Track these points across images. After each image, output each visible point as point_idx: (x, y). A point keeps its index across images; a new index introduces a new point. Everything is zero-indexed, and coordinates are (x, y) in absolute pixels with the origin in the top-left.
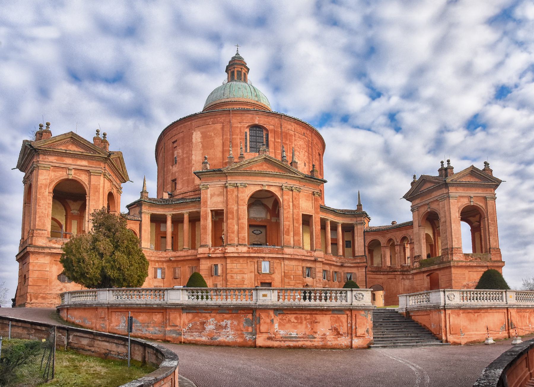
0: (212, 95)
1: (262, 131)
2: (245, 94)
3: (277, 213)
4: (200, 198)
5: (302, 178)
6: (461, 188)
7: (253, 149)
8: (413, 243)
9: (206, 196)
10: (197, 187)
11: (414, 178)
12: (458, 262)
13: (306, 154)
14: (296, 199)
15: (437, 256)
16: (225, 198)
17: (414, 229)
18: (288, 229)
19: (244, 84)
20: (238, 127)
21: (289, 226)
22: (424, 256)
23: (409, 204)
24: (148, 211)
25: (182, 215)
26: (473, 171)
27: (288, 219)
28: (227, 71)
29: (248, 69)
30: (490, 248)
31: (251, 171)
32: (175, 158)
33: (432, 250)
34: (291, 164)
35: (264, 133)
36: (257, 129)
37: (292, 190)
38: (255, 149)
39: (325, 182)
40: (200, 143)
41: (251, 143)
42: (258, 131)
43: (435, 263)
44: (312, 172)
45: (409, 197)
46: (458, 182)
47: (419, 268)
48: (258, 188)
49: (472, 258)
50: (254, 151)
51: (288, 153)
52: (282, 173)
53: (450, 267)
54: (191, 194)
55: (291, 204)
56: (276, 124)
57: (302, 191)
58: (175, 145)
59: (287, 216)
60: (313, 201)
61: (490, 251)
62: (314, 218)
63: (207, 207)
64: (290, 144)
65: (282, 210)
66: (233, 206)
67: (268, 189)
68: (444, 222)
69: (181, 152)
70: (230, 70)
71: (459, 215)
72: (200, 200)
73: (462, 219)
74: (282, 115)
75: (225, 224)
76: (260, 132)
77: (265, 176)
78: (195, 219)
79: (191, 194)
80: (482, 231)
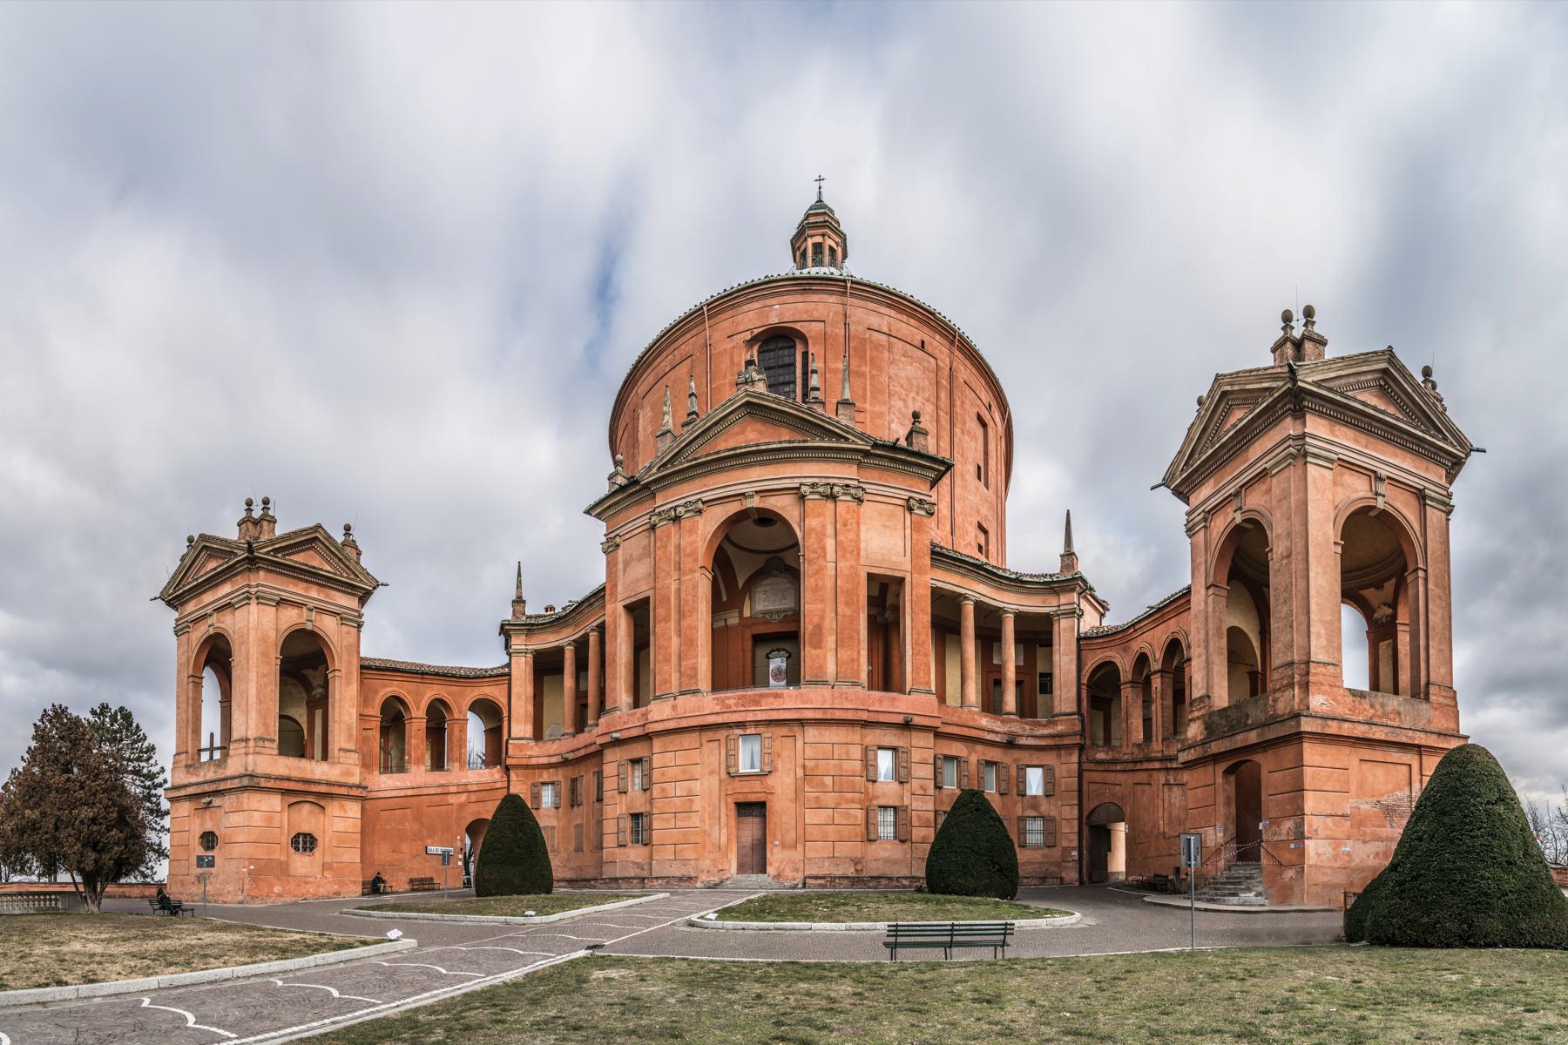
1: (794, 347)
18: (819, 627)
20: (725, 350)
21: (822, 617)
27: (820, 593)
36: (780, 345)
42: (782, 348)
51: (865, 402)
59: (817, 585)
60: (908, 531)
64: (874, 373)
68: (1283, 558)
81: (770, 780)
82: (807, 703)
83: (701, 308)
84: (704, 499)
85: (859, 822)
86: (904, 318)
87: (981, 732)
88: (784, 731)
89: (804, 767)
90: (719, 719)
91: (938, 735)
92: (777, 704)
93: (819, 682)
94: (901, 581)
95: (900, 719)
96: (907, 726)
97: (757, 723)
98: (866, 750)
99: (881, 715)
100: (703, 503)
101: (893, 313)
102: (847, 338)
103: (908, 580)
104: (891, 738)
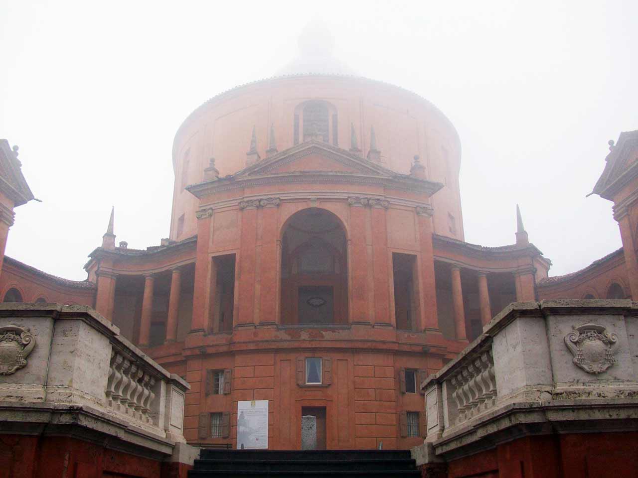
24: (111, 271)
48: (301, 207)
75: (236, 284)
81: (329, 392)
84: (282, 198)
85: (395, 423)
89: (354, 382)
94: (415, 256)
103: (418, 256)
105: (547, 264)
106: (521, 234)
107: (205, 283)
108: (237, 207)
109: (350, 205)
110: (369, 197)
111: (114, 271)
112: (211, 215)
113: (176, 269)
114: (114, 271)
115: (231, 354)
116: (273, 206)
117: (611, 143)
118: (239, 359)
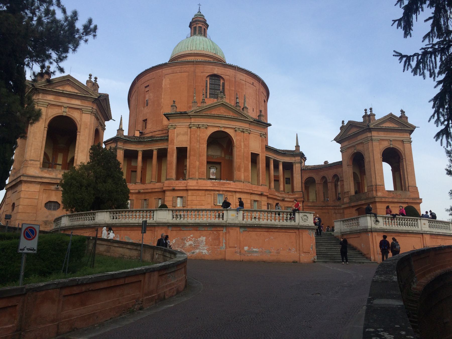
0: (178, 47)
1: (220, 80)
2: (205, 47)
3: (230, 151)
4: (168, 136)
5: (252, 122)
6: (382, 133)
7: (212, 95)
8: (343, 180)
9: (173, 135)
10: (165, 127)
11: (342, 123)
12: (381, 198)
13: (254, 101)
14: (246, 139)
15: (364, 192)
16: (189, 138)
17: (343, 167)
19: (204, 38)
22: (353, 192)
23: (339, 145)
25: (152, 151)
26: (391, 118)
28: (190, 26)
29: (208, 26)
30: (408, 187)
31: (211, 114)
32: (147, 100)
33: (359, 187)
34: (243, 109)
35: (222, 81)
36: (216, 78)
37: (244, 132)
38: (214, 95)
39: (270, 125)
40: (169, 89)
41: (210, 90)
43: (362, 198)
44: (259, 116)
45: (338, 139)
46: (379, 128)
47: (349, 203)
48: (216, 129)
49: (393, 195)
50: (213, 97)
52: (236, 116)
53: (375, 202)
54: (159, 133)
55: (242, 144)
56: (231, 75)
57: (251, 132)
58: (147, 89)
60: (260, 142)
61: (408, 189)
62: (260, 157)
63: (173, 145)
65: (235, 149)
66: (195, 145)
67: (224, 131)
69: (152, 96)
70: (193, 25)
71: (381, 156)
72: (167, 140)
73: (384, 160)
74: (236, 67)
75: (188, 160)
76: (218, 81)
77: (222, 119)
78: (163, 154)
79: (159, 133)
80: (401, 171)
82: (237, 187)
83: (194, 61)
86: (249, 77)
87: (276, 197)
88: (230, 194)
90: (212, 188)
91: (268, 198)
92: (229, 186)
93: (240, 181)
94: (259, 154)
95: (260, 193)
96: (261, 195)
97: (223, 191)
98: (251, 200)
99: (255, 191)
100: (208, 125)
101: (246, 75)
102: (235, 81)
103: (260, 155)
104: (257, 198)
105: (305, 159)
106: (297, 146)
107: (172, 158)
108: (188, 126)
109: (236, 131)
110: (243, 128)
111: (124, 147)
112: (175, 128)
113: (156, 149)
114: (124, 147)
115: (187, 190)
116: (204, 128)
117: (343, 122)
118: (190, 192)
